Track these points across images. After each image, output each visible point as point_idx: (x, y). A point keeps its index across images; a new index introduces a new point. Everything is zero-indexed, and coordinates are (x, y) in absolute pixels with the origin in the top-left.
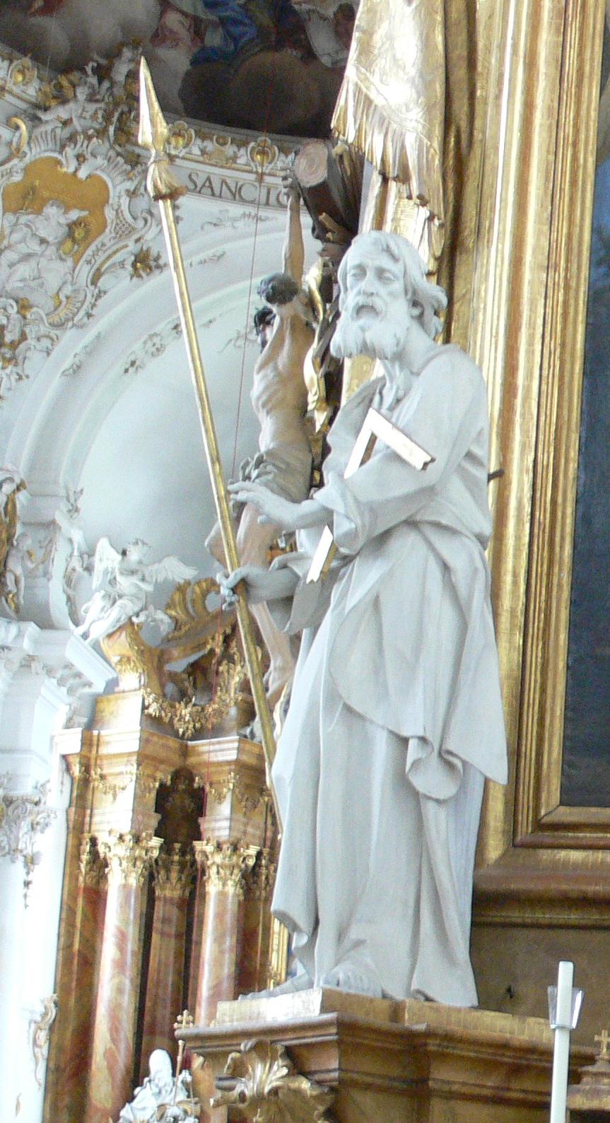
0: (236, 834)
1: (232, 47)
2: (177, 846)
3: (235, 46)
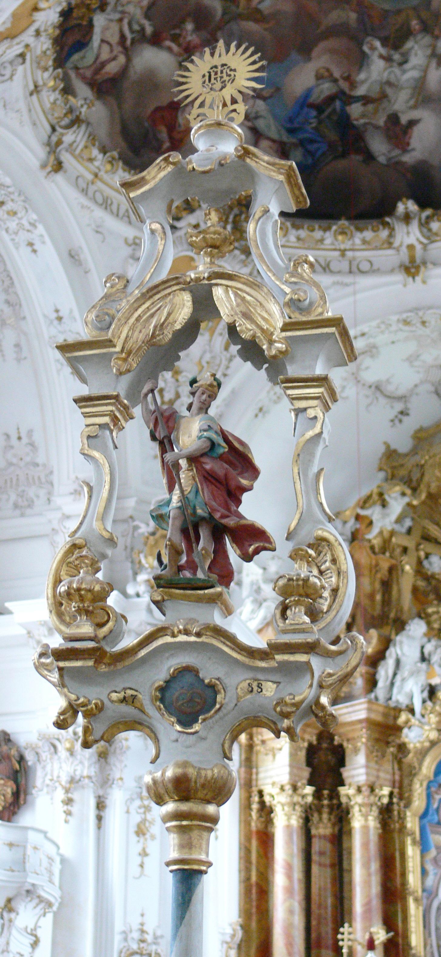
0: (372, 779)
2: (326, 792)
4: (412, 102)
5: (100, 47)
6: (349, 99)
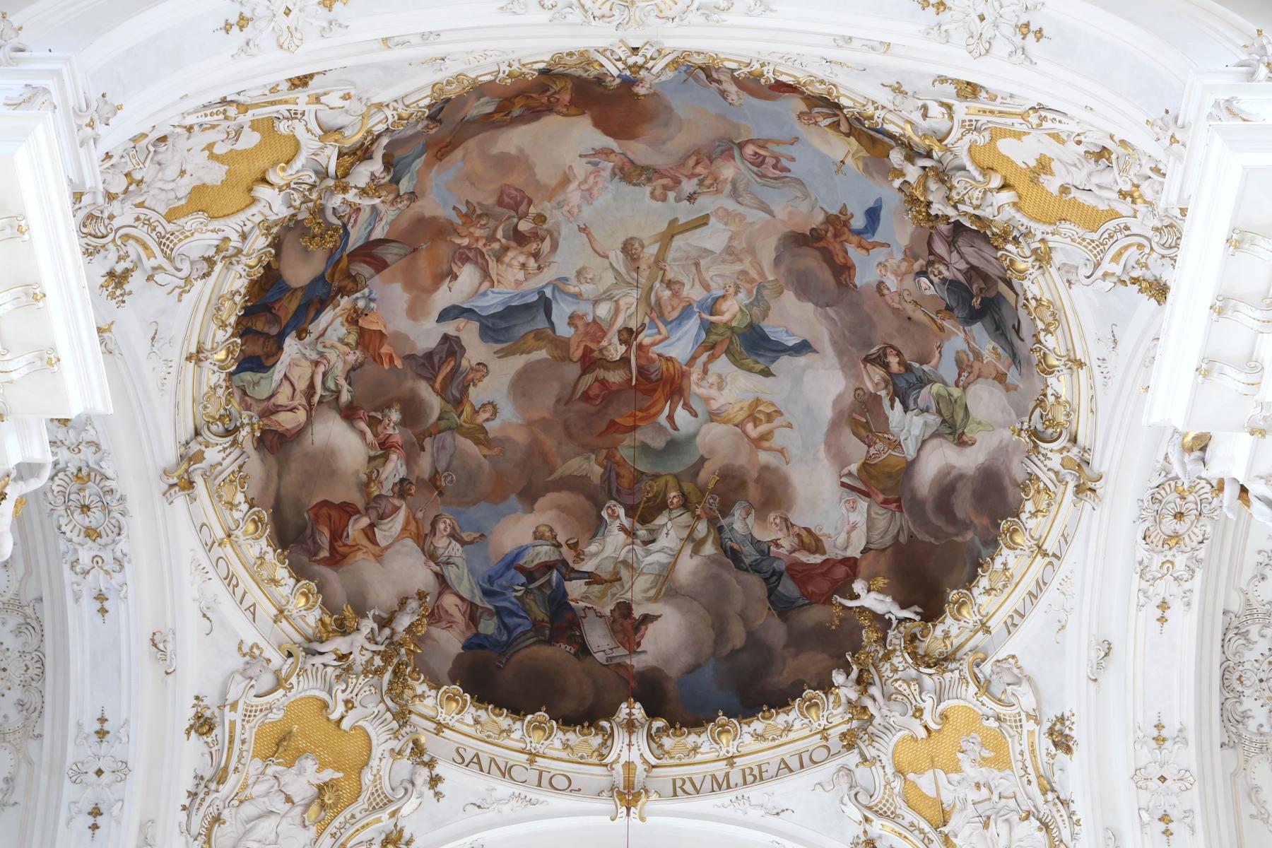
1: (505, 638)
3: (509, 637)
4: (652, 593)
5: (280, 385)
6: (570, 573)
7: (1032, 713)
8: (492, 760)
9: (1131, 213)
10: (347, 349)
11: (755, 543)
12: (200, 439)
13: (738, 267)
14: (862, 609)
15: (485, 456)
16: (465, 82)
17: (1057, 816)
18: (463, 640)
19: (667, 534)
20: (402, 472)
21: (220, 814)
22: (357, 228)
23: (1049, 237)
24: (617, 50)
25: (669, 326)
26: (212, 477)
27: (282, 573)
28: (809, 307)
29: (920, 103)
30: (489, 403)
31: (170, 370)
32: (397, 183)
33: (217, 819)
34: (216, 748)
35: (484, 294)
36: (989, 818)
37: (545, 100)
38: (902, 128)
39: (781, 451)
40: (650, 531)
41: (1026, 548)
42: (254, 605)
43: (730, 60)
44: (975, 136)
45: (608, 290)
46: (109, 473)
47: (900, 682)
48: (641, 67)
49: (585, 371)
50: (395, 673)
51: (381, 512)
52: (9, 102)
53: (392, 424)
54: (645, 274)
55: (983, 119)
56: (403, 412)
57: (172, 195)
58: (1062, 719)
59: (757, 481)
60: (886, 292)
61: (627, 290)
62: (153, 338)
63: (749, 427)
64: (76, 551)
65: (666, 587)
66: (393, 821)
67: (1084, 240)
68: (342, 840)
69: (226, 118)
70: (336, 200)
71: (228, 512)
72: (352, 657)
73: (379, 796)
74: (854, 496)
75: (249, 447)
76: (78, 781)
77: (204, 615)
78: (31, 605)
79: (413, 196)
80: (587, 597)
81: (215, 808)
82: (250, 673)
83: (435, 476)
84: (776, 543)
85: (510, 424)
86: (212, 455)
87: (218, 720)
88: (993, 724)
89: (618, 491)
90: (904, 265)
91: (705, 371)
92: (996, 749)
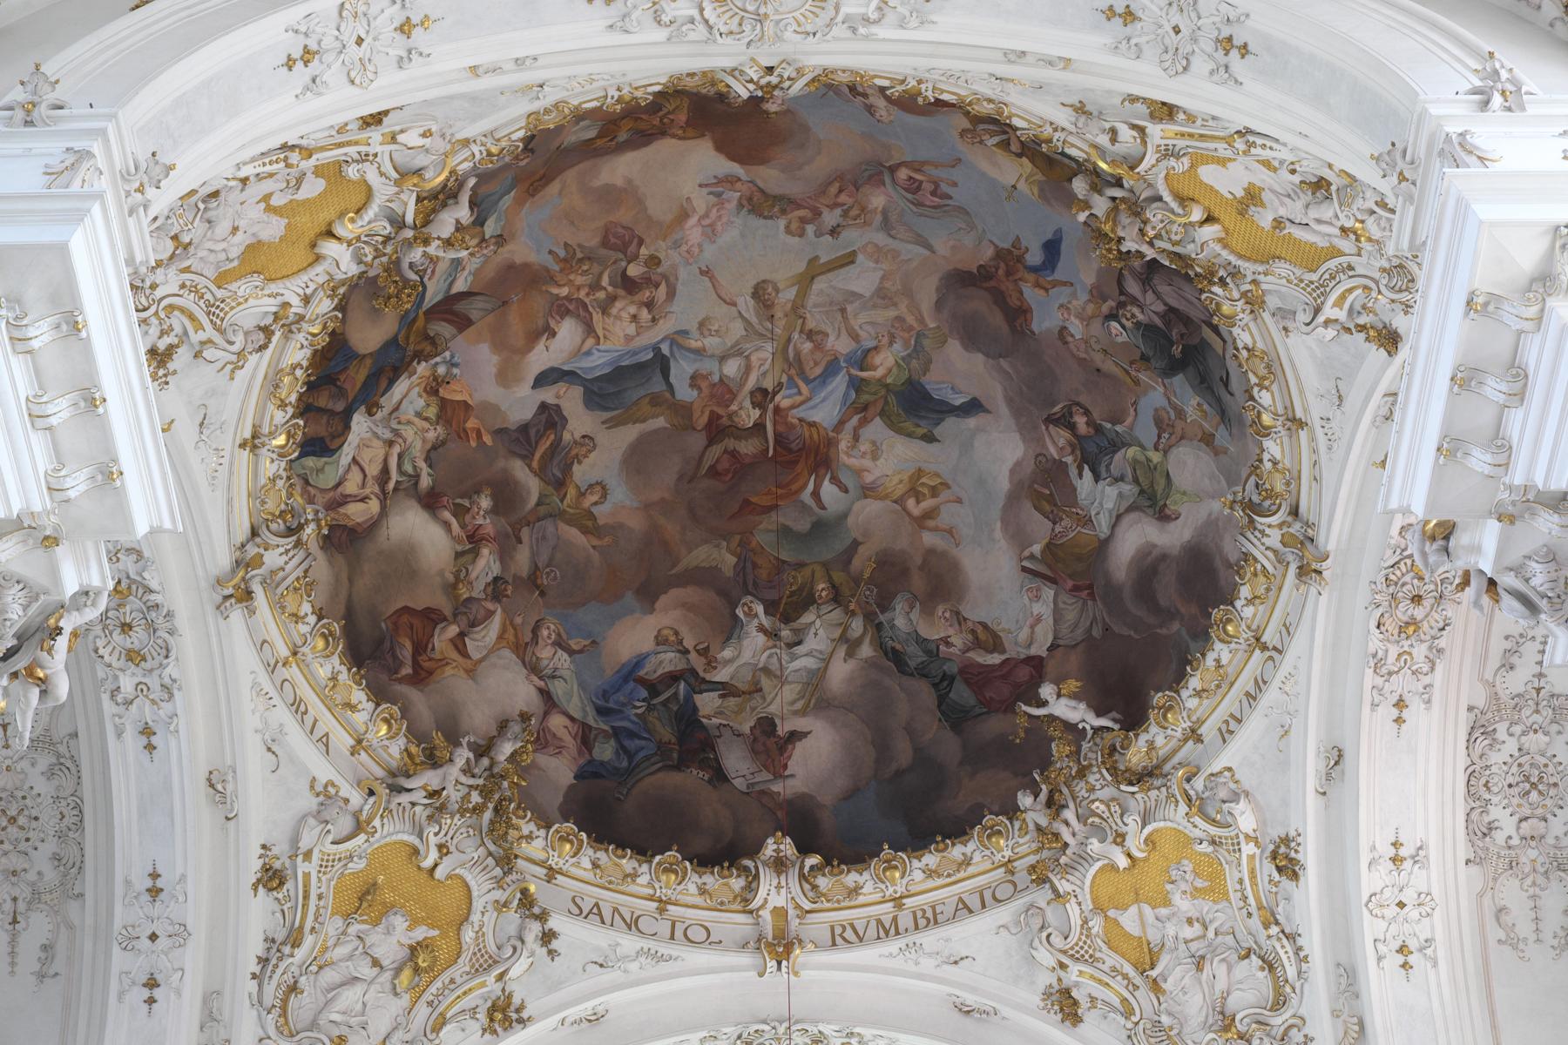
1: (625, 764)
4: (799, 705)
6: (701, 685)
7: (1252, 834)
8: (616, 910)
9: (1354, 251)
10: (426, 425)
11: (921, 641)
12: (258, 540)
13: (892, 313)
14: (1052, 718)
15: (594, 547)
16: (567, 111)
17: (1281, 952)
18: (575, 769)
19: (816, 634)
20: (496, 569)
21: (296, 982)
22: (435, 280)
23: (1261, 278)
24: (748, 71)
25: (811, 385)
26: (273, 585)
27: (359, 696)
28: (979, 358)
29: (1107, 126)
30: (597, 483)
31: (222, 461)
32: (482, 225)
33: (293, 988)
34: (289, 905)
35: (588, 353)
36: (1203, 957)
37: (656, 122)
38: (1086, 153)
39: (950, 532)
40: (795, 631)
41: (1242, 641)
42: (327, 735)
43: (881, 77)
44: (1173, 162)
45: (737, 343)
46: (154, 585)
47: (1097, 804)
48: (776, 87)
49: (711, 441)
50: (496, 810)
51: (471, 617)
52: (49, 171)
53: (482, 513)
54: (781, 323)
55: (1181, 143)
56: (495, 497)
57: (223, 256)
58: (1286, 840)
59: (921, 568)
60: (1070, 339)
61: (759, 343)
62: (201, 424)
63: (911, 503)
64: (116, 678)
65: (816, 697)
66: (499, 985)
67: (1302, 281)
68: (441, 1009)
69: (288, 166)
70: (416, 254)
71: (293, 625)
72: (445, 793)
73: (482, 956)
74: (1038, 582)
75: (314, 546)
76: (130, 947)
77: (269, 749)
78: (65, 741)
79: (501, 240)
80: (721, 713)
81: (290, 974)
82: (326, 815)
83: (535, 573)
84: (946, 641)
85: (623, 507)
86: (273, 559)
87: (289, 872)
88: (1205, 847)
89: (755, 584)
90: (1090, 308)
91: (856, 438)
92: (1210, 878)
